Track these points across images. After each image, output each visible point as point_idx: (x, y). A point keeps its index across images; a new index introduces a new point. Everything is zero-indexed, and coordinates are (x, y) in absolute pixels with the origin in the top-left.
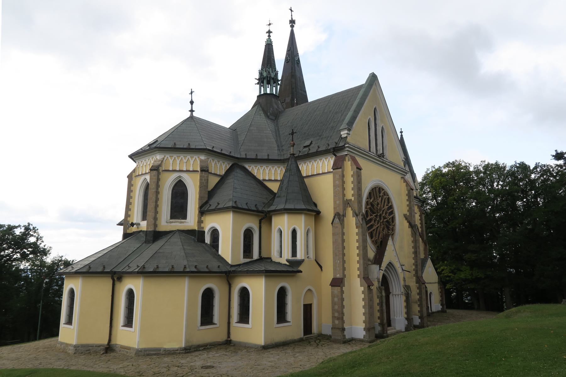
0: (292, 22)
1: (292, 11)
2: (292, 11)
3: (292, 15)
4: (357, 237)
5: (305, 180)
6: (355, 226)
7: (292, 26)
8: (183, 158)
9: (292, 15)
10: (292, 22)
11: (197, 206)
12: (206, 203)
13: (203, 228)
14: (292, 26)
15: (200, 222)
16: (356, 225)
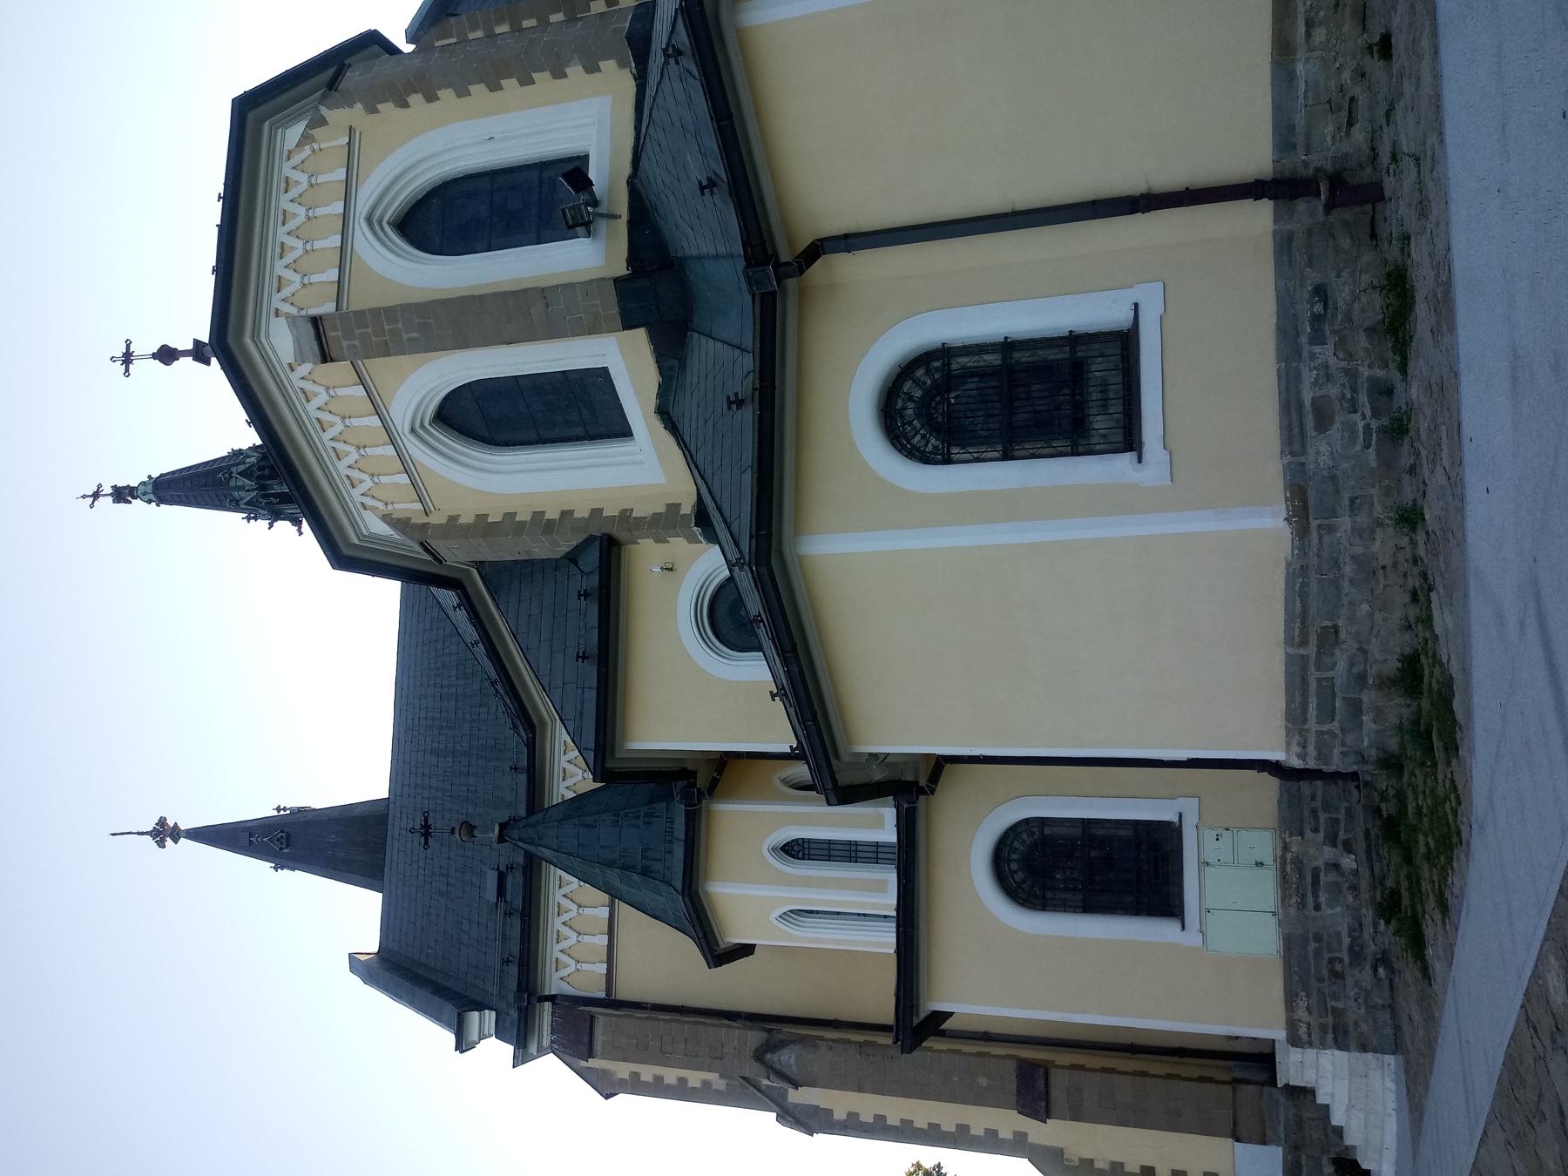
0: (164, 833)
3: (139, 833)
7: (176, 834)
9: (139, 833)
10: (164, 833)
14: (176, 834)
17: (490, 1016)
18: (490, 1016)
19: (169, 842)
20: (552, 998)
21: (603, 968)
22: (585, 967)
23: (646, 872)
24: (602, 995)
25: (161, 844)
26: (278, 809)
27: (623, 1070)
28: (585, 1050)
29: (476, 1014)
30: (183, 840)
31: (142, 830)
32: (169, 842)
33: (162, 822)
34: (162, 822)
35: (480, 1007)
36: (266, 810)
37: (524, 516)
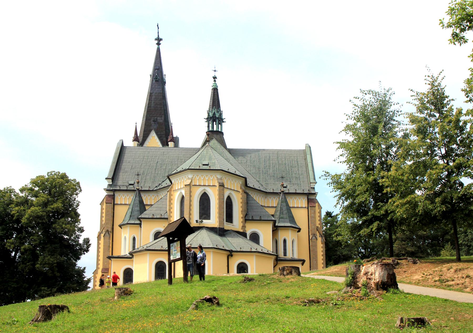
0: (159, 40)
1: (158, 28)
2: (158, 28)
3: (158, 32)
4: (322, 249)
5: (292, 210)
6: (321, 243)
7: (158, 44)
8: (201, 176)
9: (158, 32)
10: (159, 40)
11: (242, 216)
12: (246, 215)
13: (246, 231)
14: (158, 44)
15: (244, 227)
16: (321, 242)
17: (111, 183)
18: (111, 183)
19: (157, 42)
20: (114, 195)
21: (119, 203)
22: (119, 200)
23: (131, 216)
24: (115, 203)
25: (156, 40)
26: (165, 75)
27: (104, 207)
28: (107, 202)
29: (111, 181)
30: (157, 46)
31: (159, 33)
32: (157, 42)
33: (161, 40)
34: (161, 40)
35: (112, 181)
36: (165, 72)
37: (172, 206)
